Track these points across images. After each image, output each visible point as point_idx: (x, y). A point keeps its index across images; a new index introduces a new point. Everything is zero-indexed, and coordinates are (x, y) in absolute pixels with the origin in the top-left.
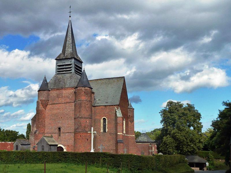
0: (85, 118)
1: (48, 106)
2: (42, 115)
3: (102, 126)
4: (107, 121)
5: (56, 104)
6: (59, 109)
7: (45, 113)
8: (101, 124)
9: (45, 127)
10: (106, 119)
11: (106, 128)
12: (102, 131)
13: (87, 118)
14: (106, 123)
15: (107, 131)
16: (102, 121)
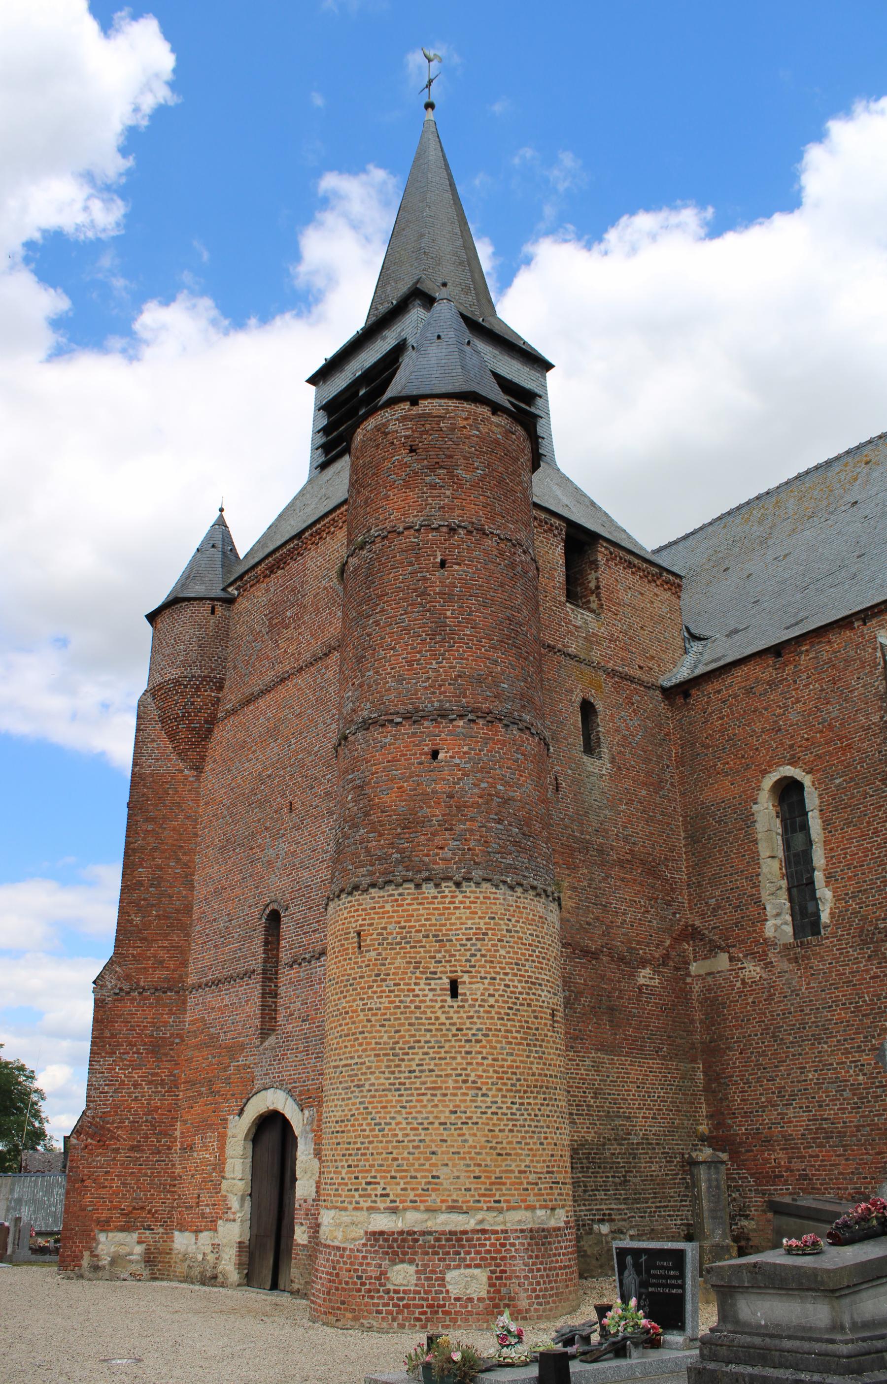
0: (413, 717)
1: (217, 734)
2: (165, 818)
3: (771, 867)
4: (812, 799)
5: (263, 693)
6: (273, 733)
7: (196, 801)
8: (764, 851)
9: (185, 929)
10: (807, 781)
11: (819, 876)
12: (779, 924)
13: (443, 714)
14: (805, 827)
15: (825, 917)
16: (765, 812)
